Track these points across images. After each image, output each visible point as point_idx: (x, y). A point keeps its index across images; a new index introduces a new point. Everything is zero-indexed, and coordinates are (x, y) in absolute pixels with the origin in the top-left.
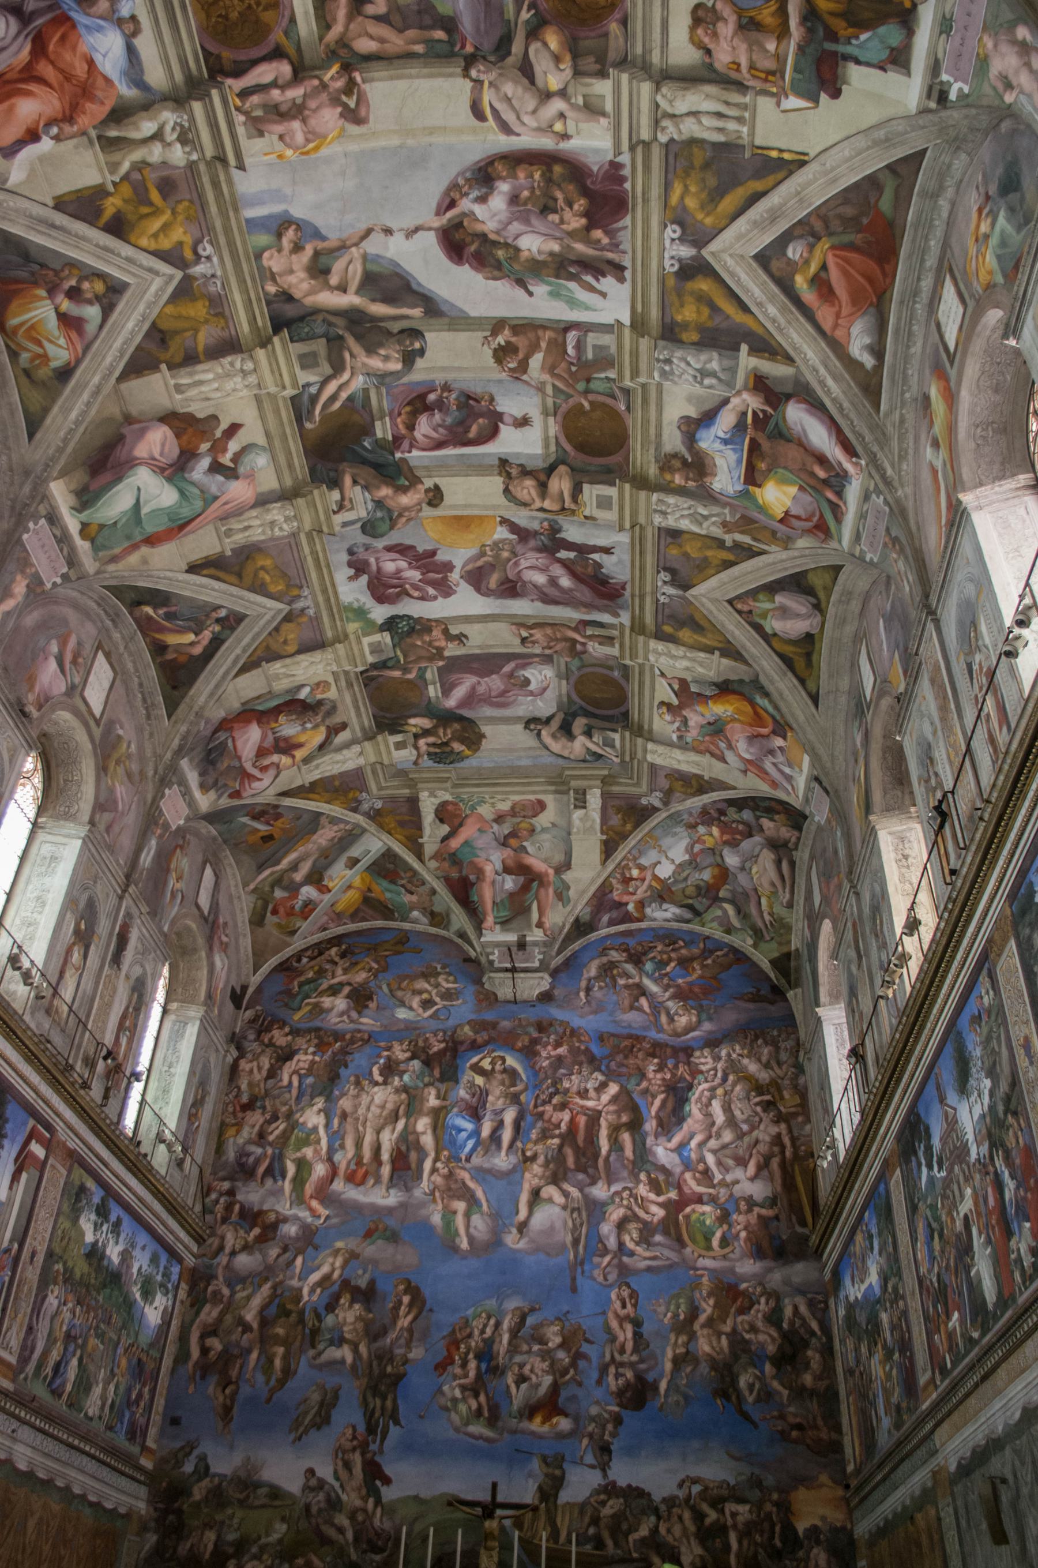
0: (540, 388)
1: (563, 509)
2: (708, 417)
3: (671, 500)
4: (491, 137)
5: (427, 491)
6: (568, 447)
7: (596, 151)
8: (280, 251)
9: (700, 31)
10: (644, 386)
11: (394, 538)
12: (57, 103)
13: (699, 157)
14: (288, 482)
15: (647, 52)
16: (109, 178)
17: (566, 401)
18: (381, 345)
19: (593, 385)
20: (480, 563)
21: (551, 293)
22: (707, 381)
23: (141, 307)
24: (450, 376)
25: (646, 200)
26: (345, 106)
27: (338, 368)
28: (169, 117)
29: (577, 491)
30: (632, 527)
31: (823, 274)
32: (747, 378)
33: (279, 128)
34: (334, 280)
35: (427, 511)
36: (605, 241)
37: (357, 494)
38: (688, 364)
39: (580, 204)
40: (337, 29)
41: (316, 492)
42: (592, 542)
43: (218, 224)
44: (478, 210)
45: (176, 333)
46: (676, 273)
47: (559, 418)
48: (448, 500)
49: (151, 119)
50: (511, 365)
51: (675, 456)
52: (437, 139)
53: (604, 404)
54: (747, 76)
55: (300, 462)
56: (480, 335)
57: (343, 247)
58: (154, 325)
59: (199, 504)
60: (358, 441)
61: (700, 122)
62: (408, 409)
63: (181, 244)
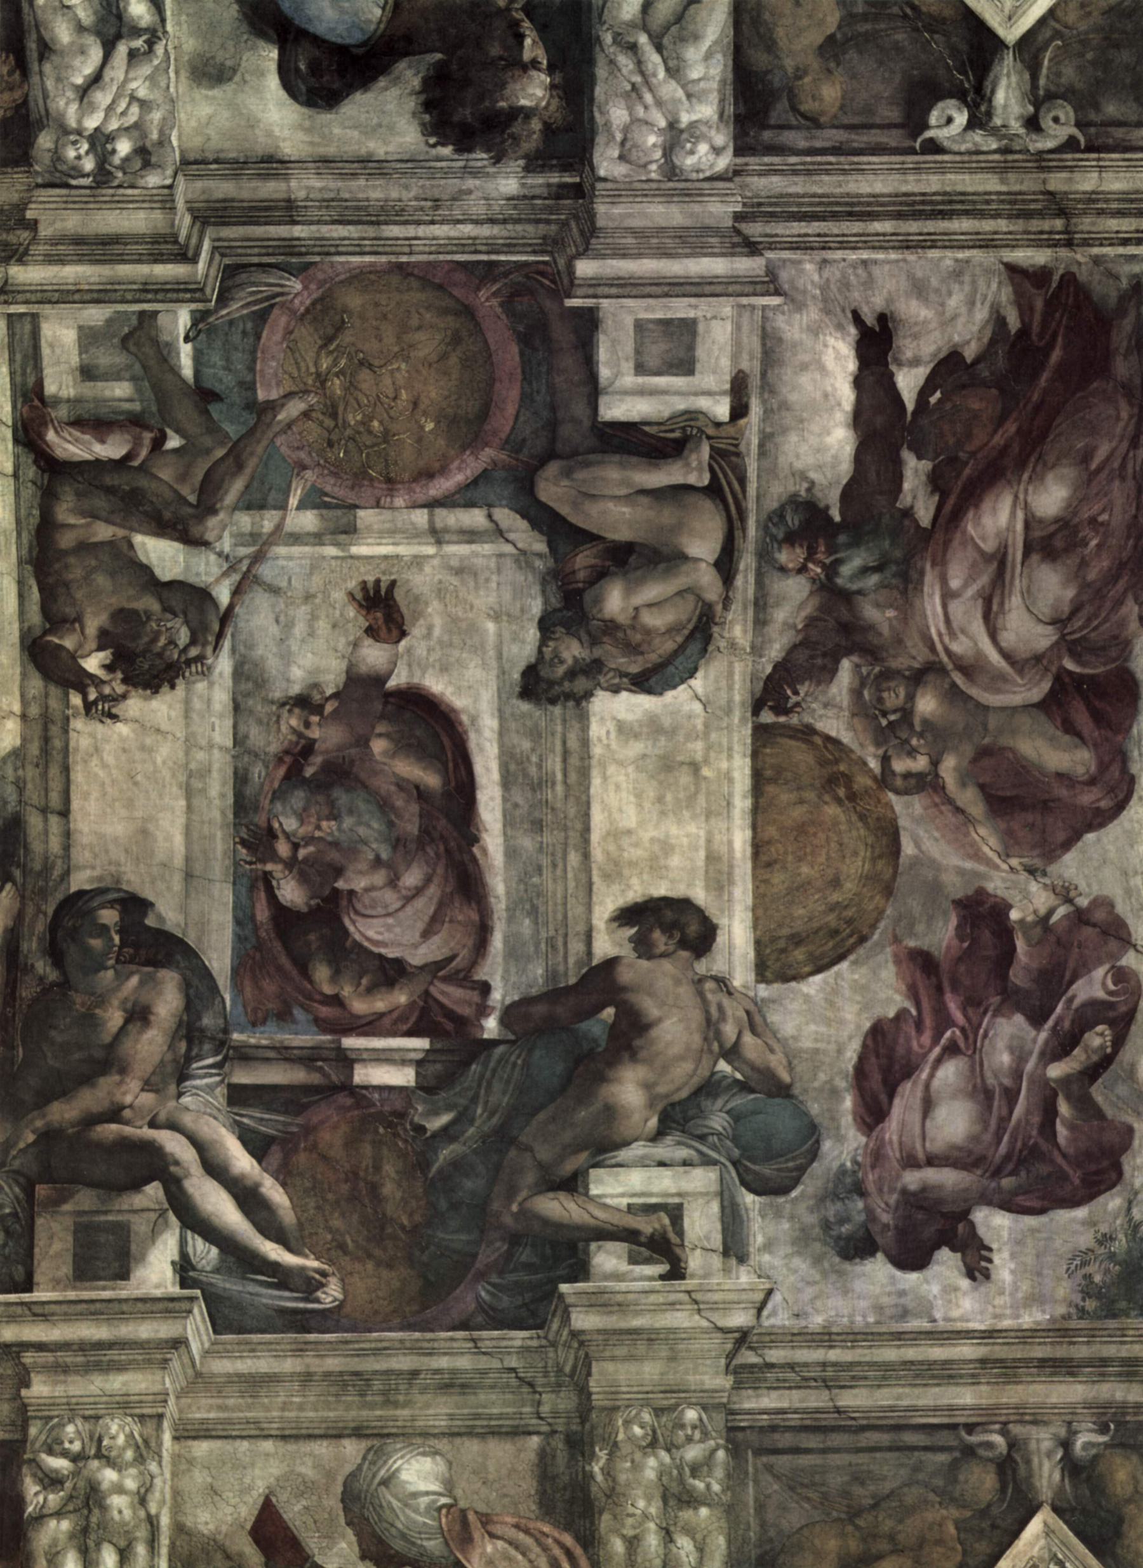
1: (714, 490)
30: (752, 248)
38: (96, 79)
42: (846, 395)
50: (183, 636)
62: (322, 973)
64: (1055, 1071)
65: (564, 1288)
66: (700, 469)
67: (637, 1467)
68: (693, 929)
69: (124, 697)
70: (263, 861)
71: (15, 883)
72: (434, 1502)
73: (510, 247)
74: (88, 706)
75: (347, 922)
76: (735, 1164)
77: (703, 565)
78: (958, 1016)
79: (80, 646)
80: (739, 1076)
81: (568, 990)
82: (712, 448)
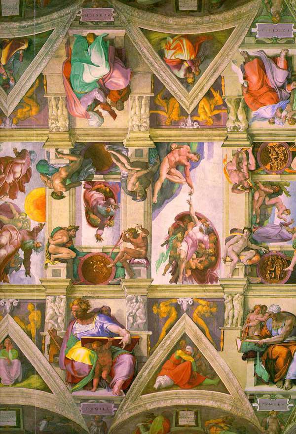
0: (116, 246)
2: (112, 320)
8: (189, 152)
10: (123, 291)
11: (35, 175)
14: (78, 132)
17: (110, 257)
18: (141, 183)
19: (120, 271)
20: (14, 212)
22: (131, 318)
23: (180, 94)
27: (133, 164)
31: (182, 361)
32: (137, 335)
33: (234, 162)
34: (173, 170)
35: (49, 192)
37: (66, 161)
38: (137, 310)
40: (263, 188)
41: (70, 143)
43: (204, 132)
45: (167, 105)
50: (127, 235)
55: (89, 139)
57: (186, 176)
59: (78, 90)
60: (94, 166)
62: (108, 190)
64: (4, 175)
68: (54, 195)
78: (17, 183)
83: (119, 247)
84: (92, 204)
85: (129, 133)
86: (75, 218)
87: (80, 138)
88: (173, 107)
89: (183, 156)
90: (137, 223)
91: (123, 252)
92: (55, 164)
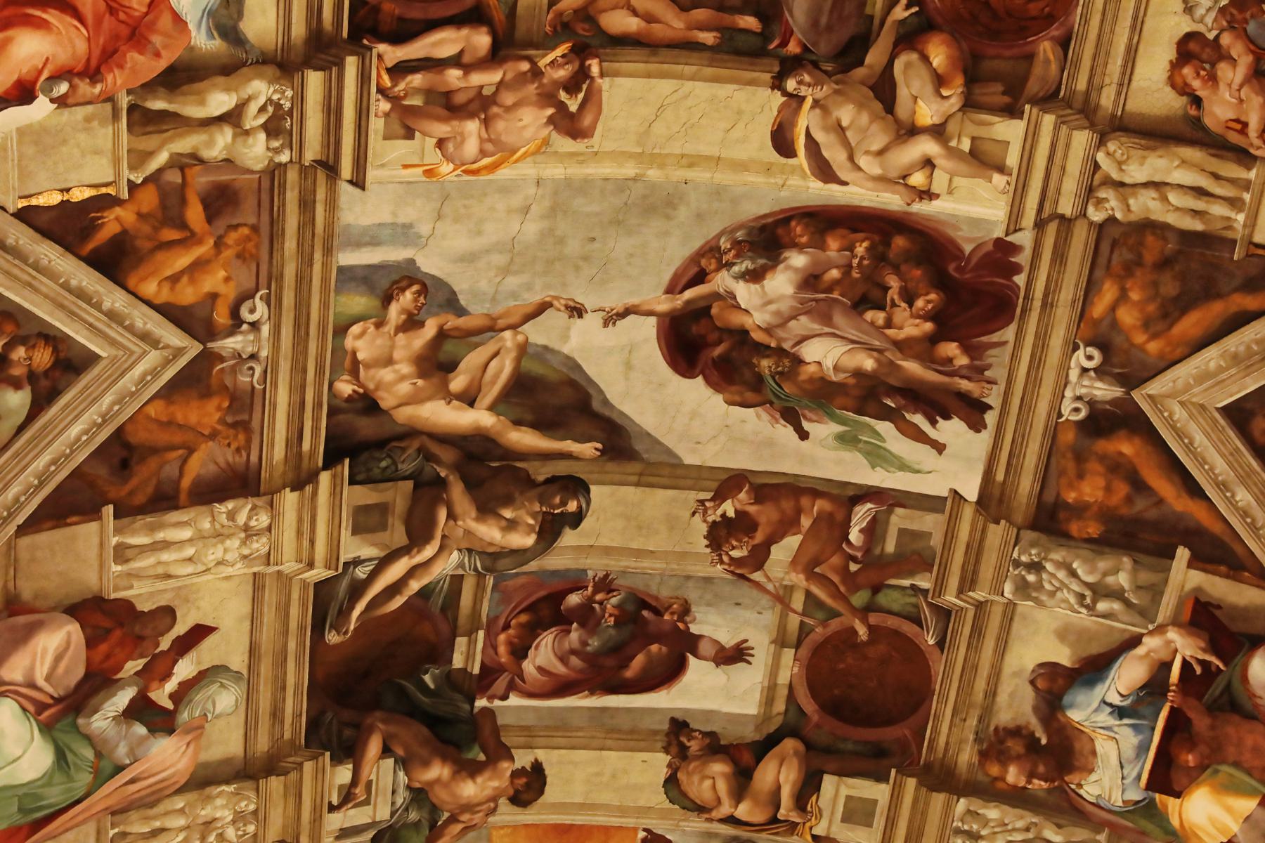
0: (782, 598)
1: (774, 820)
3: (993, 813)
4: (795, 181)
5: (515, 774)
6: (809, 706)
7: (976, 222)
8: (379, 325)
9: (1187, 71)
10: (980, 606)
12: (81, 47)
13: (1153, 249)
14: (263, 744)
15: (1094, 87)
16: (126, 174)
17: (824, 623)
18: (508, 501)
21: (840, 438)
22: (1102, 606)
23: (107, 400)
24: (615, 564)
25: (1047, 305)
26: (562, 106)
27: (419, 533)
28: (261, 89)
29: (808, 788)
32: (1181, 602)
33: (442, 129)
34: (458, 382)
35: (508, 814)
36: (962, 361)
38: (1073, 574)
39: (927, 301)
41: (308, 766)
44: (745, 293)
45: (155, 450)
46: (1080, 425)
47: (804, 651)
48: (552, 793)
49: (227, 90)
50: (736, 554)
51: (1017, 732)
52: (700, 175)
53: (896, 633)
54: (1257, 142)
55: (295, 705)
56: (693, 496)
57: (491, 328)
58: (120, 431)
59: (84, 779)
60: (415, 673)
61: (1164, 199)
63: (214, 296)
65: (328, 754)
66: (788, 815)
67: (224, 807)
68: (525, 797)
69: (705, 521)
70: (594, 586)
71: (599, 456)
72: (210, 712)
73: (931, 747)
74: (702, 502)
75: (553, 629)
76: (390, 825)
77: (733, 810)
79: (738, 500)
80: (439, 823)
81: (498, 737)
82: (798, 824)
83: (786, 586)
84: (581, 671)
85: (277, 568)
86: (632, 732)
87: (287, 735)
88: (170, 424)
89: (392, 347)
90: (688, 513)
91: (810, 574)
92: (393, 803)
